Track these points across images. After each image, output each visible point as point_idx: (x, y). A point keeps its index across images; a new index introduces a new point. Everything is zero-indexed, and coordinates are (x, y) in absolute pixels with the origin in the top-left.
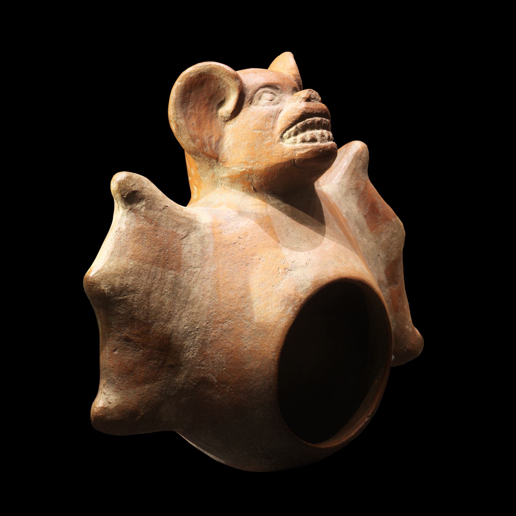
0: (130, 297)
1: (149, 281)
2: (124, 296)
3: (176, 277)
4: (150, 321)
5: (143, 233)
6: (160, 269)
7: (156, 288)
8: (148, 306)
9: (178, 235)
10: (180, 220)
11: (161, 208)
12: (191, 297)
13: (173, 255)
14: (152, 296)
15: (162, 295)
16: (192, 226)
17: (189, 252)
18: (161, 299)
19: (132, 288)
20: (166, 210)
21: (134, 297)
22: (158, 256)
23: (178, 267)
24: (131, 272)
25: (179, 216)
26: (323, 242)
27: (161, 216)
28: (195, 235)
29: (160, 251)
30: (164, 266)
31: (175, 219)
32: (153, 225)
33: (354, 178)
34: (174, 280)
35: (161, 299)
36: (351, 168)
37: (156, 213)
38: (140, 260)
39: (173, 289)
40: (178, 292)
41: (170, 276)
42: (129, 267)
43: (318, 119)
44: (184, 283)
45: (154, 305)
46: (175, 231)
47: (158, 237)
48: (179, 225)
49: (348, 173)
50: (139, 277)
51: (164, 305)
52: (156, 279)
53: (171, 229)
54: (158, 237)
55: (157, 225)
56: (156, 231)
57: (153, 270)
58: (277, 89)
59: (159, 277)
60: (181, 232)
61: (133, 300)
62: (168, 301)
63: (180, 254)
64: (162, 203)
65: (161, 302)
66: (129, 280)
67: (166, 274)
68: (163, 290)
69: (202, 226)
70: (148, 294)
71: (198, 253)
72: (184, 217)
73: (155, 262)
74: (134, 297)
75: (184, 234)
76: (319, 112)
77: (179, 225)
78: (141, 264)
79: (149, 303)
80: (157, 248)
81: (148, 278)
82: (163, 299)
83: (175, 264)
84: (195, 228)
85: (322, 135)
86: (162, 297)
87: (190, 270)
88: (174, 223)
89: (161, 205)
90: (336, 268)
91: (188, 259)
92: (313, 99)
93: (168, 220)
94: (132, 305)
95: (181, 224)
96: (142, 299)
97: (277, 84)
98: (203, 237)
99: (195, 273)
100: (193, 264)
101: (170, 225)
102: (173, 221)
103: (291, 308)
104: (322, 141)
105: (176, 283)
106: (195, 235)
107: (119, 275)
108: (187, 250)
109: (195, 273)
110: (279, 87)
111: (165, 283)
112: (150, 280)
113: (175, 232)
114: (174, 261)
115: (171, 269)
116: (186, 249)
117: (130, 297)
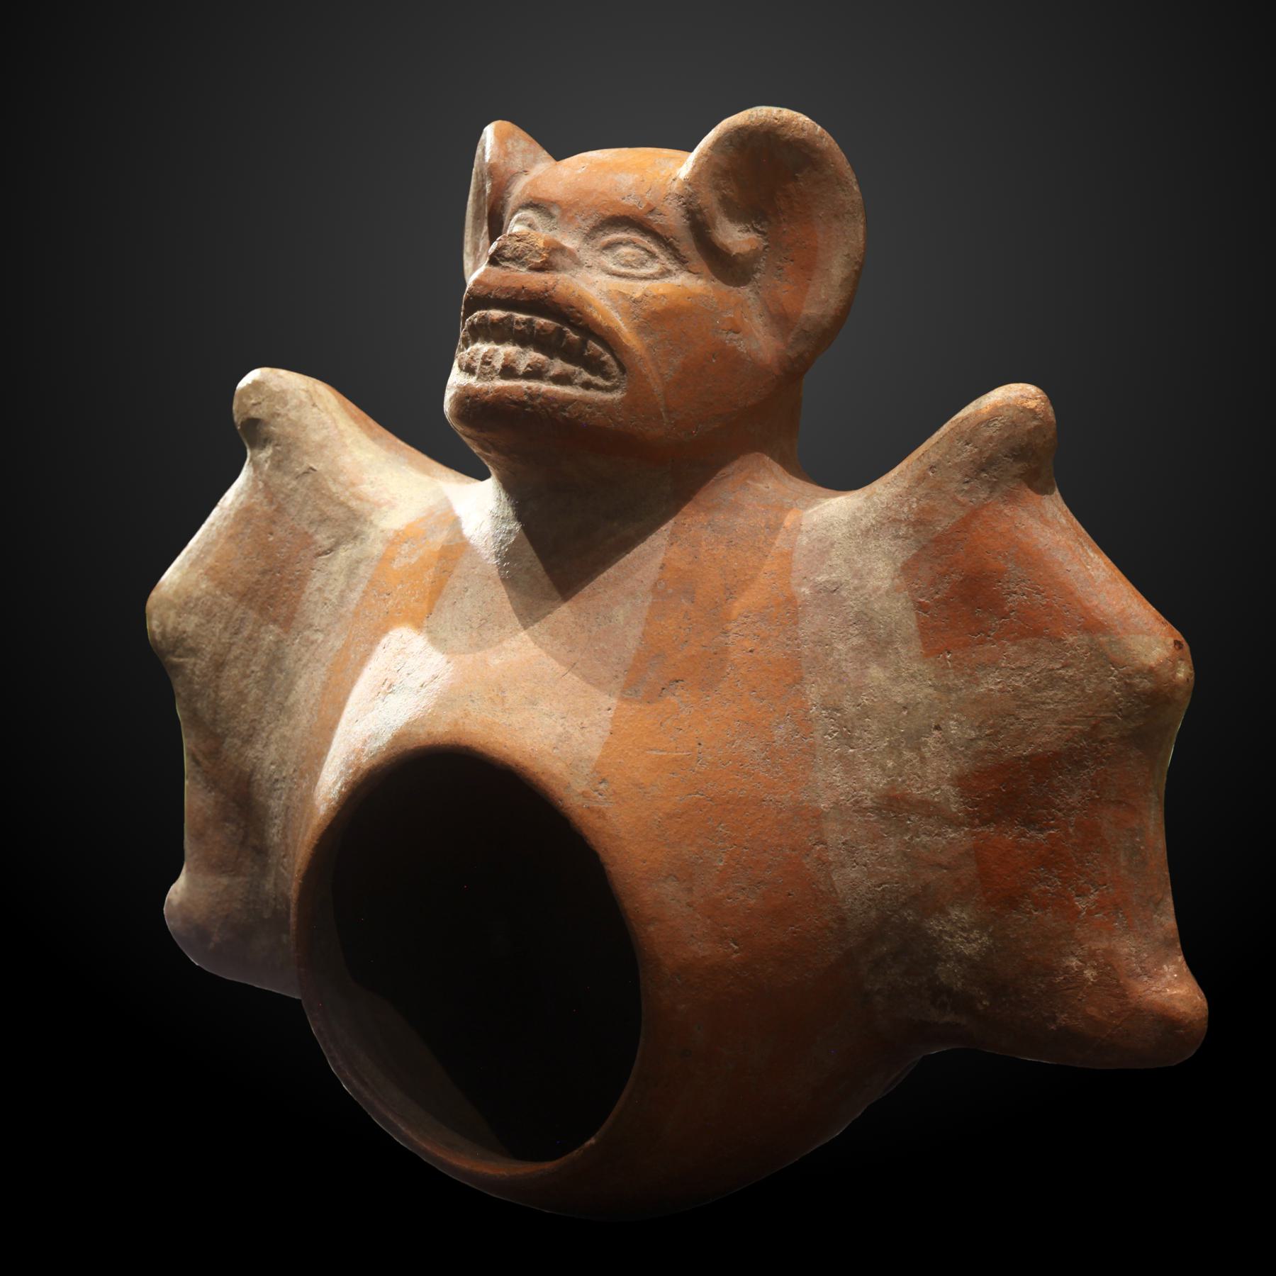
0: (189, 661)
1: (226, 638)
2: (180, 656)
3: (278, 642)
4: (219, 730)
5: (248, 522)
6: (253, 615)
7: (237, 658)
8: (216, 692)
9: (315, 543)
10: (332, 511)
11: (299, 470)
12: (292, 699)
13: (287, 589)
14: (225, 674)
15: (245, 676)
16: (351, 529)
17: (319, 589)
18: (242, 685)
19: (191, 643)
20: (309, 479)
21: (195, 664)
22: (258, 582)
23: (287, 623)
24: (196, 605)
25: (331, 499)
26: (505, 644)
27: (295, 490)
28: (348, 553)
29: (264, 573)
30: (262, 610)
31: (321, 503)
32: (274, 507)
33: (920, 491)
34: (274, 648)
35: (242, 685)
36: (925, 460)
37: (286, 479)
38: (220, 583)
39: (267, 669)
40: (274, 679)
41: (270, 635)
42: (196, 593)
43: (496, 314)
44: (288, 663)
45: (227, 694)
46: (311, 531)
47: (271, 539)
48: (324, 520)
49: (909, 475)
50: (209, 622)
51: (244, 701)
52: (240, 636)
53: (304, 525)
54: (271, 539)
55: (280, 510)
56: (274, 522)
57: (238, 614)
58: (551, 216)
59: (246, 633)
60: (323, 538)
61: (193, 673)
62: (254, 693)
63: (301, 589)
64: (306, 458)
65: (240, 693)
66: (190, 623)
67: (263, 629)
68: (248, 666)
69: (372, 537)
70: (219, 665)
71: (333, 597)
72: (342, 504)
73: (247, 596)
74: (195, 664)
75: (327, 544)
76: (503, 296)
77: (324, 520)
78: (218, 593)
79: (217, 686)
80: (261, 564)
81: (225, 629)
82: (246, 686)
83: (284, 610)
84: (356, 537)
85: (486, 362)
86: (245, 682)
87: (307, 633)
88: (316, 513)
89: (301, 464)
90: (467, 715)
91: (312, 606)
92: (508, 260)
93: (305, 502)
94: (190, 682)
95: (328, 518)
96: (205, 675)
97: (554, 203)
98: (358, 562)
99: (312, 643)
100: (316, 621)
101: (305, 515)
102: (315, 507)
103: (337, 788)
104: (483, 376)
105: (275, 658)
106: (348, 553)
107: (174, 606)
108: (318, 585)
109: (312, 643)
110: (556, 212)
111: (255, 651)
112: (227, 635)
113: (311, 537)
114: (284, 603)
115: (275, 621)
116: (317, 581)
117: (189, 661)
